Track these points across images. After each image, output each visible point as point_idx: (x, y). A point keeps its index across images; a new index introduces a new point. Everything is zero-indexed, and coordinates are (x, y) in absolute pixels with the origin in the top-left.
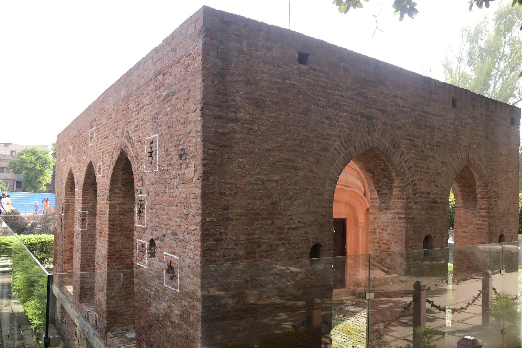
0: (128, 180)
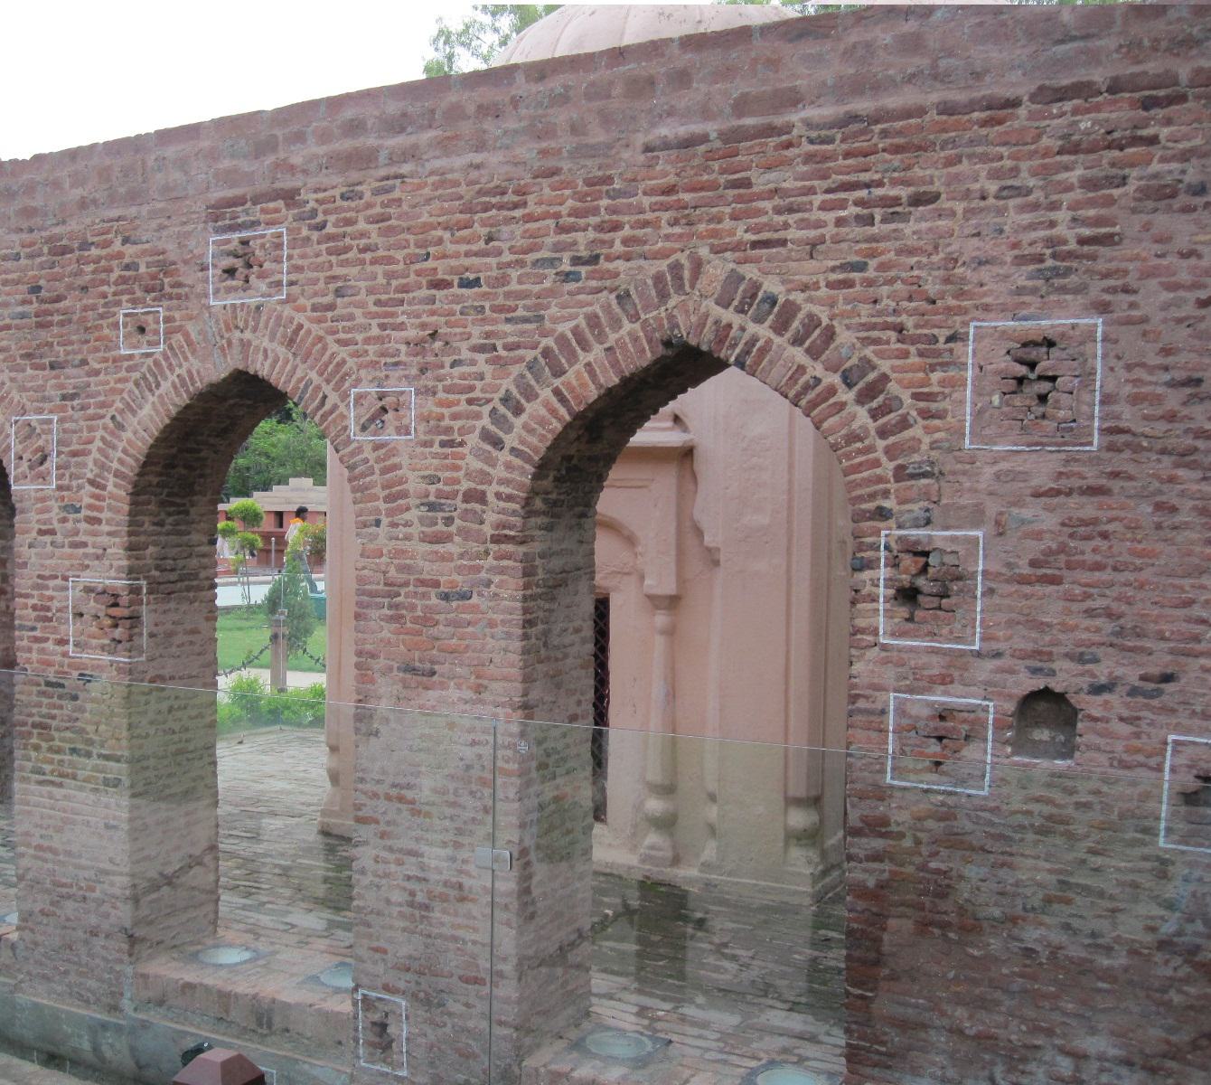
0: (575, 461)
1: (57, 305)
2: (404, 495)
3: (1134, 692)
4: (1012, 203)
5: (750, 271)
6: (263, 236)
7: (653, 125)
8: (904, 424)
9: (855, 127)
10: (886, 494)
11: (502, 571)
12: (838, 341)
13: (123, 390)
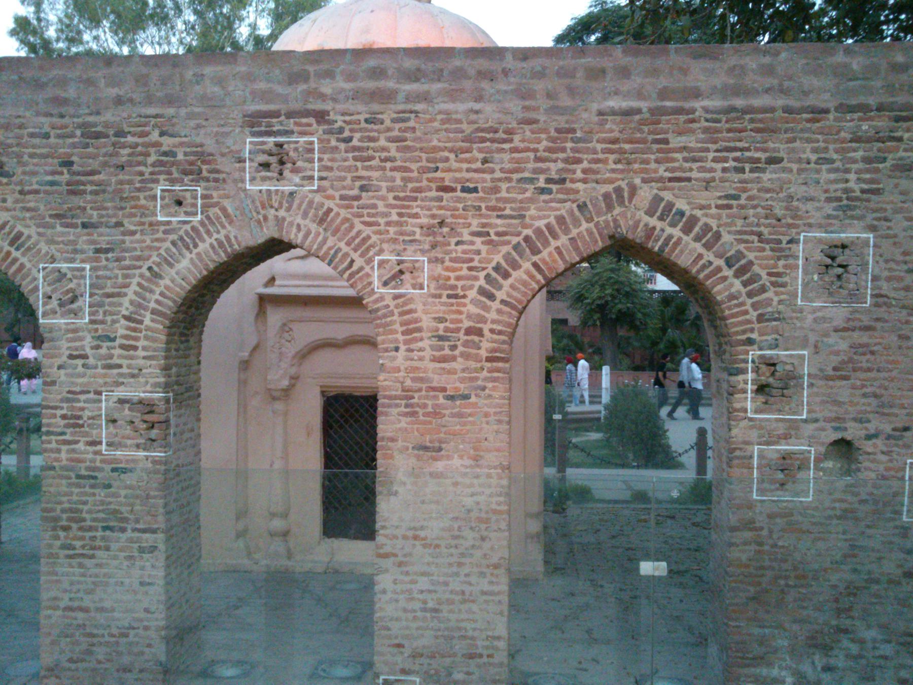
1: (91, 178)
2: (419, 330)
3: (889, 437)
4: (824, 167)
5: (667, 196)
6: (297, 142)
7: (605, 99)
8: (763, 290)
9: (733, 115)
10: (752, 330)
11: (495, 380)
12: (723, 240)
13: (160, 248)
